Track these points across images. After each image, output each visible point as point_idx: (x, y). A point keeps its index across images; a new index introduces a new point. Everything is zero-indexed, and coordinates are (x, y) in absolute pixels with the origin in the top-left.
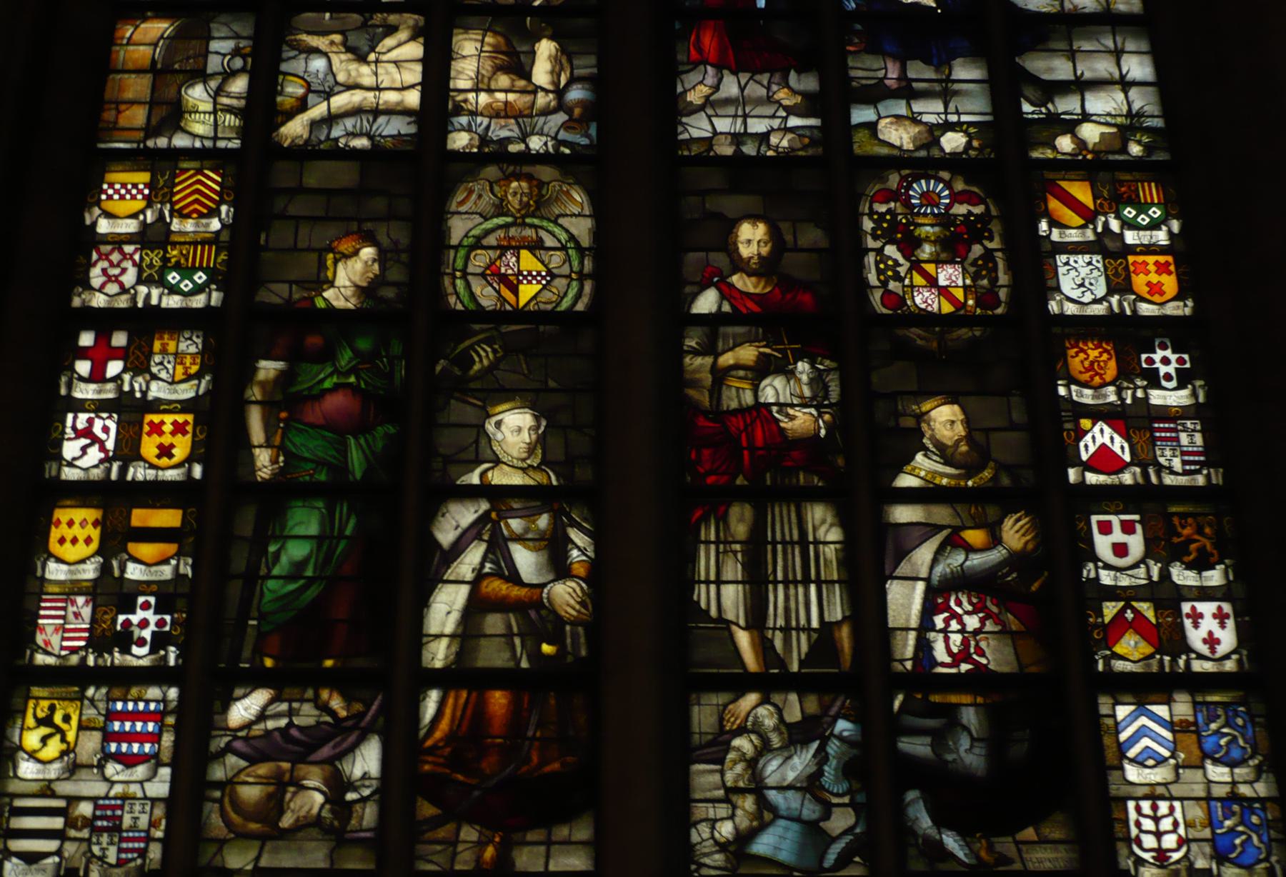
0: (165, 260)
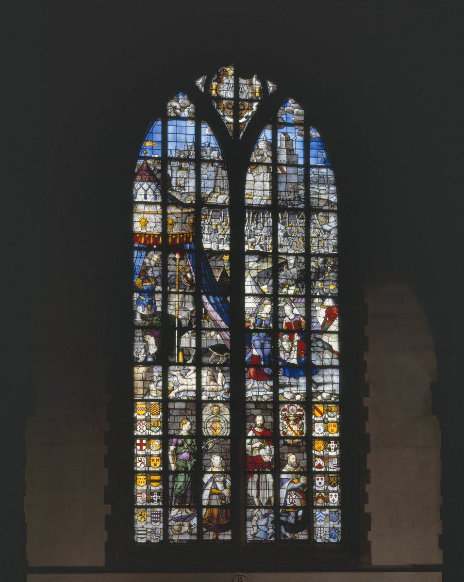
0: (151, 425)
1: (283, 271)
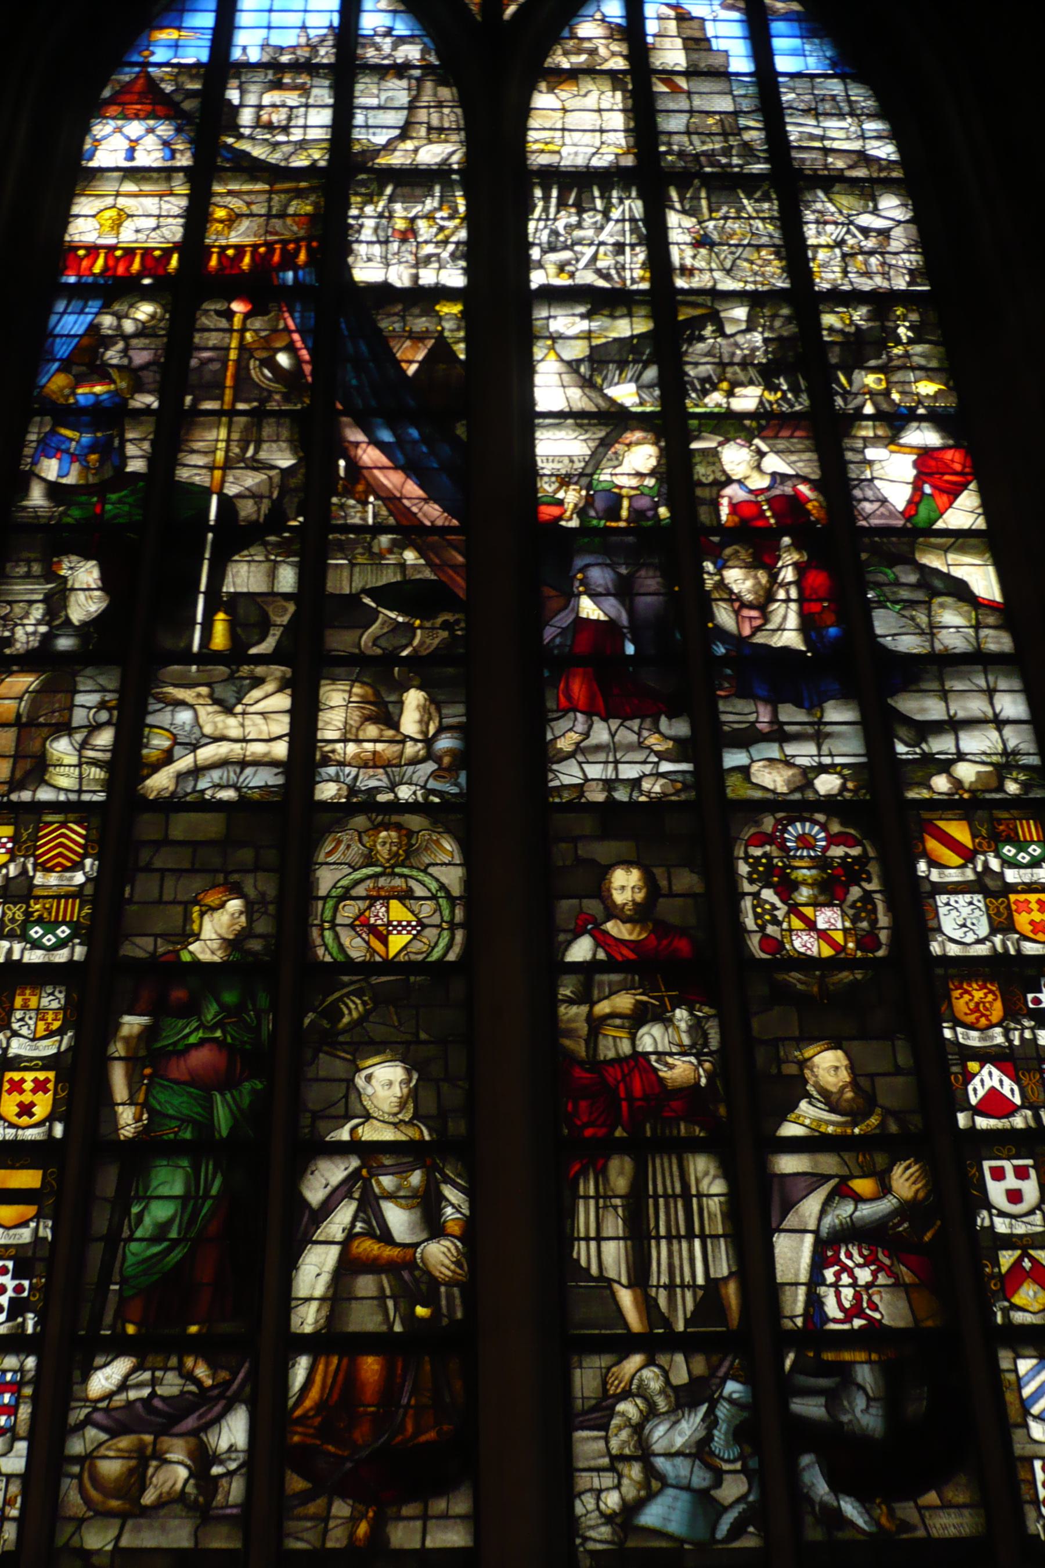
0: (28, 914)
1: (702, 339)
